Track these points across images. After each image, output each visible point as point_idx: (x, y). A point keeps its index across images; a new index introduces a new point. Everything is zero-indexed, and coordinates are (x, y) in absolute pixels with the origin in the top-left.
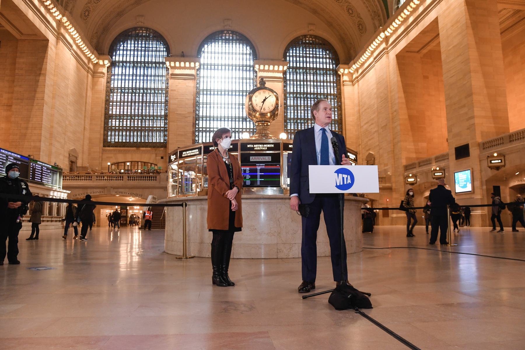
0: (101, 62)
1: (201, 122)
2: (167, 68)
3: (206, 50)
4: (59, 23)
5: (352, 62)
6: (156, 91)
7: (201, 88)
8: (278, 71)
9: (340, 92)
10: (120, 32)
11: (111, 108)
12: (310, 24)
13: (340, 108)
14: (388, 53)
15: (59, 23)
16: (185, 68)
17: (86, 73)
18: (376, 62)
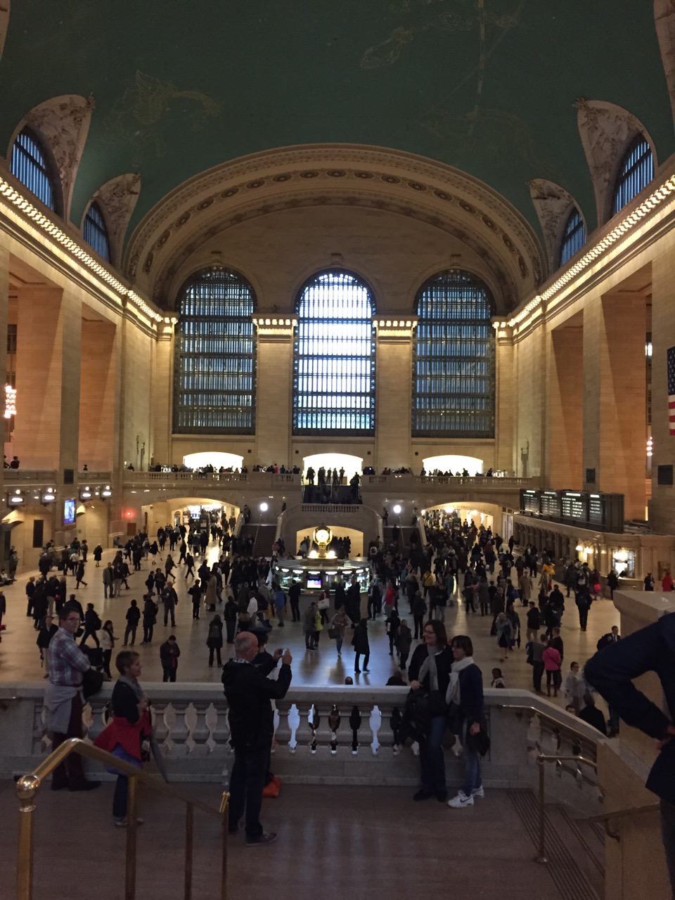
0: (167, 320)
1: (300, 398)
2: (254, 325)
3: (306, 298)
5: (510, 315)
6: (239, 356)
7: (301, 353)
8: (405, 328)
9: (495, 354)
11: (181, 378)
12: (453, 256)
13: (492, 376)
14: (544, 323)
15: (125, 299)
16: (278, 327)
17: (149, 338)
18: (534, 328)
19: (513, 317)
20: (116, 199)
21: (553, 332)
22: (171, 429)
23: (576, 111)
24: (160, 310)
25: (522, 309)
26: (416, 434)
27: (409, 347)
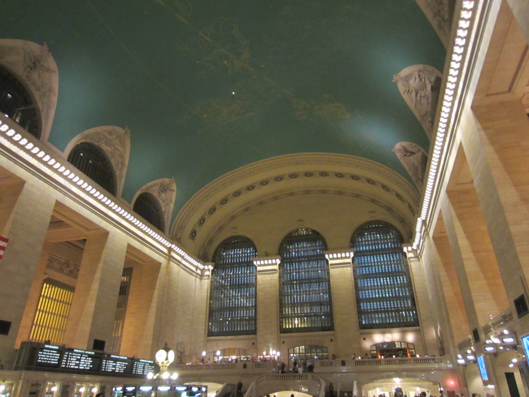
0: (206, 267)
4: (170, 249)
5: (412, 241)
8: (346, 258)
10: (220, 242)
13: (410, 284)
14: (428, 234)
15: (170, 249)
16: (268, 265)
19: (414, 242)
20: (163, 195)
21: (433, 238)
22: (206, 336)
23: (396, 83)
24: (201, 261)
25: (415, 232)
26: (362, 327)
27: (349, 270)
